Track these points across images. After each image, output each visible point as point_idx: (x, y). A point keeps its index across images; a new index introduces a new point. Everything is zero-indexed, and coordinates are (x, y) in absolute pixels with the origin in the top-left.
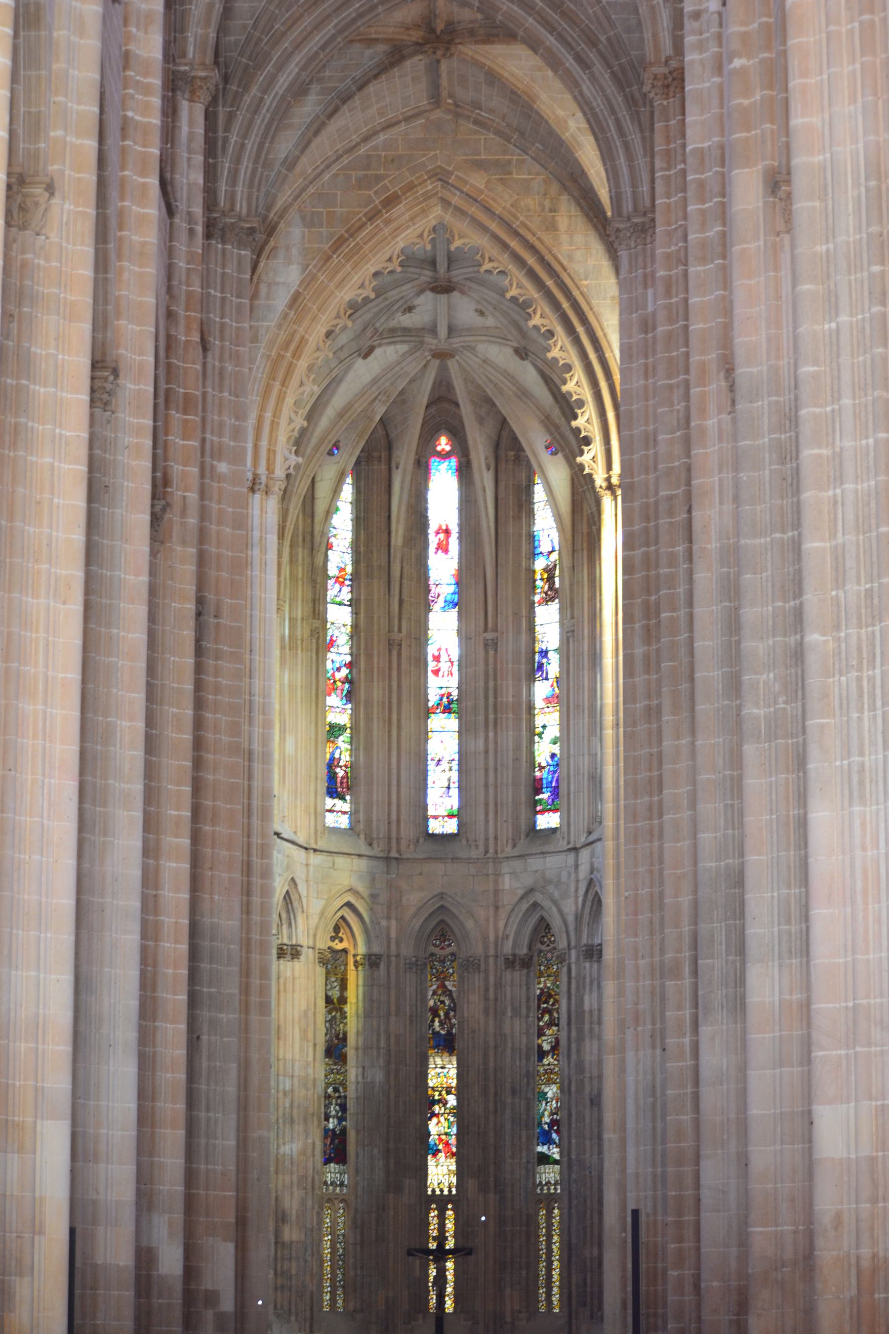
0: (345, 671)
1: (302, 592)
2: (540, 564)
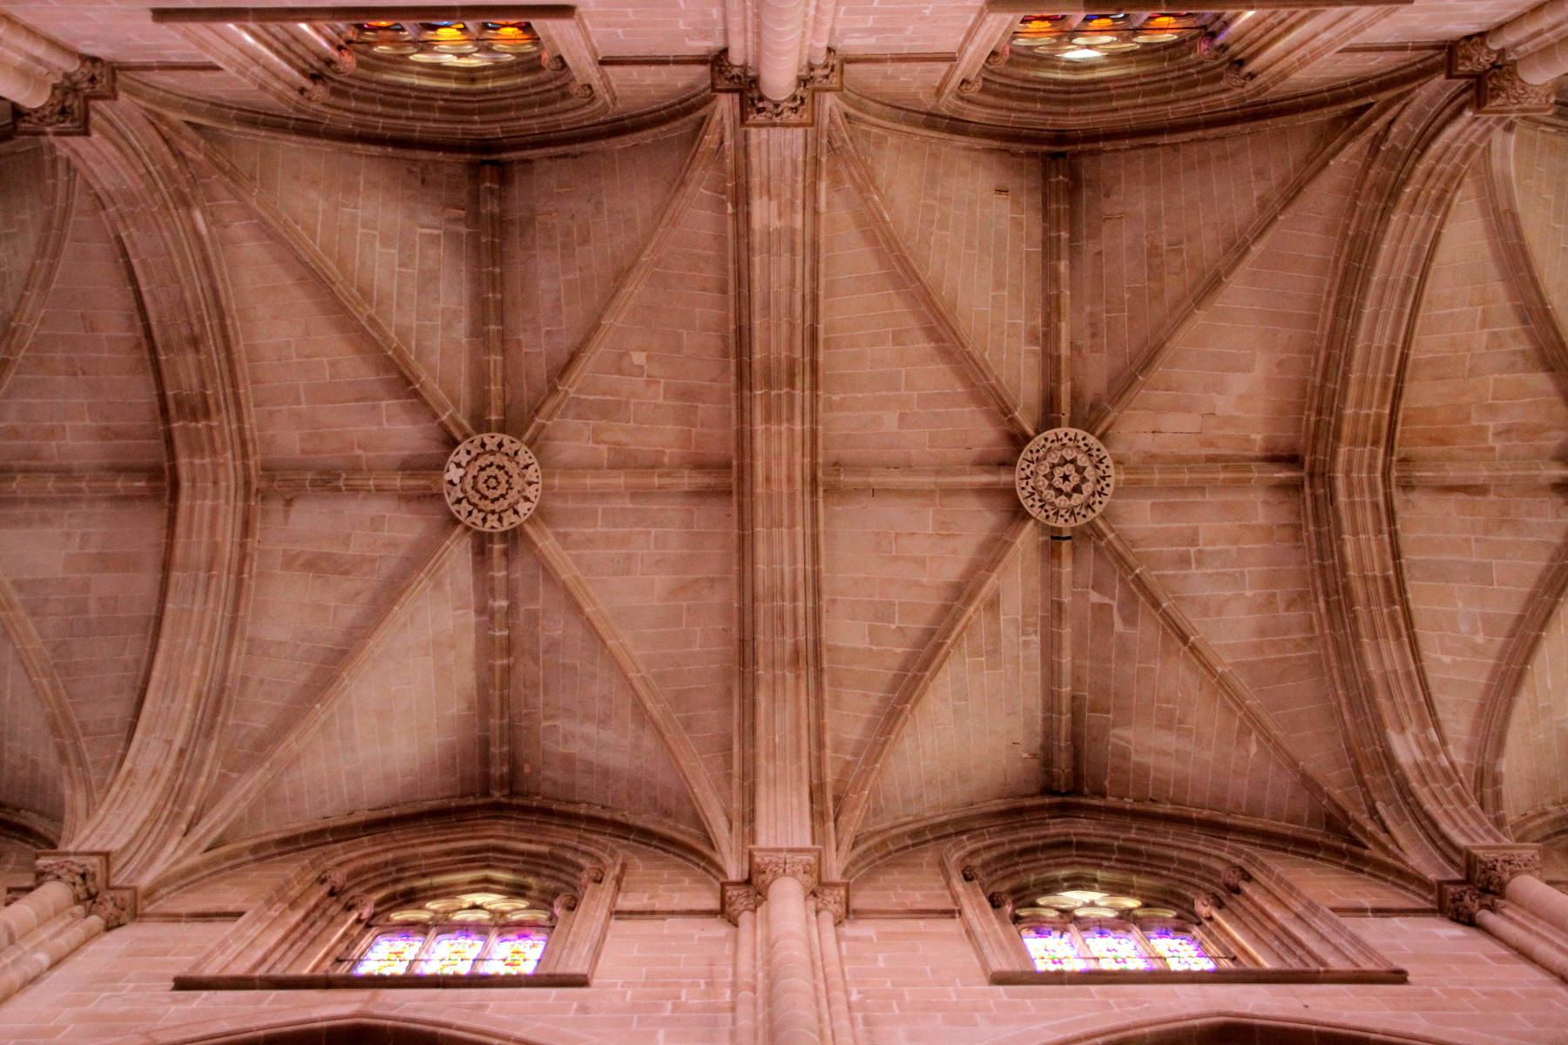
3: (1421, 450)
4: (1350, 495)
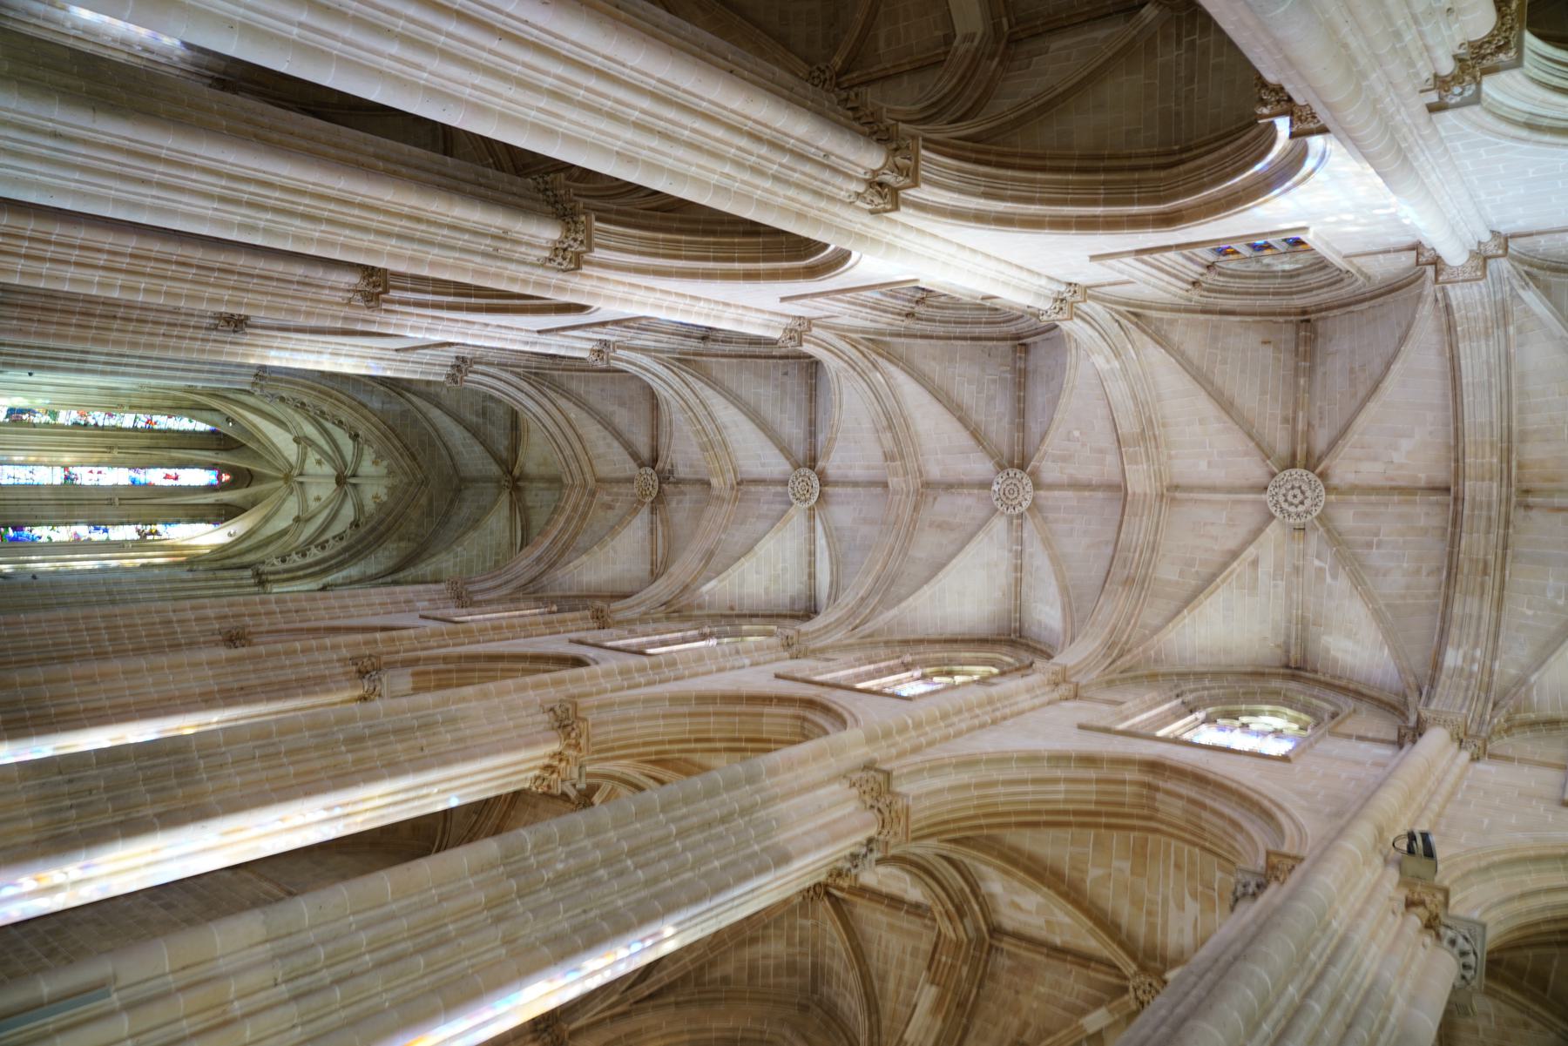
0: (92, 422)
1: (146, 402)
2: (160, 527)
3: (1537, 485)
4: (1473, 509)
